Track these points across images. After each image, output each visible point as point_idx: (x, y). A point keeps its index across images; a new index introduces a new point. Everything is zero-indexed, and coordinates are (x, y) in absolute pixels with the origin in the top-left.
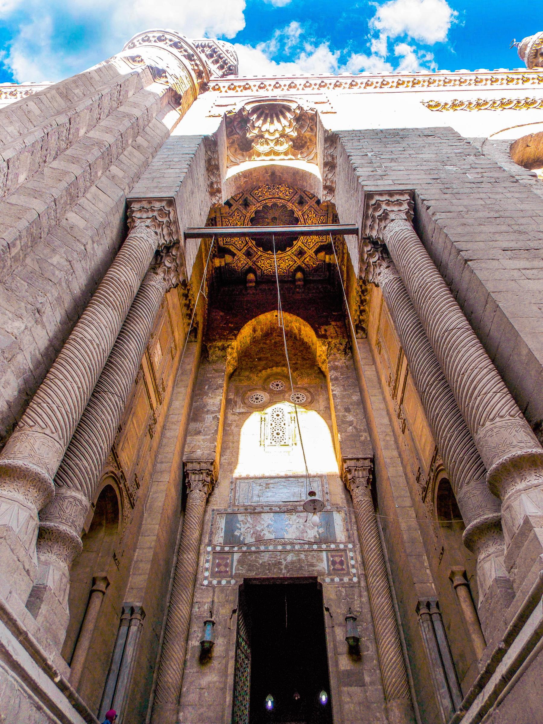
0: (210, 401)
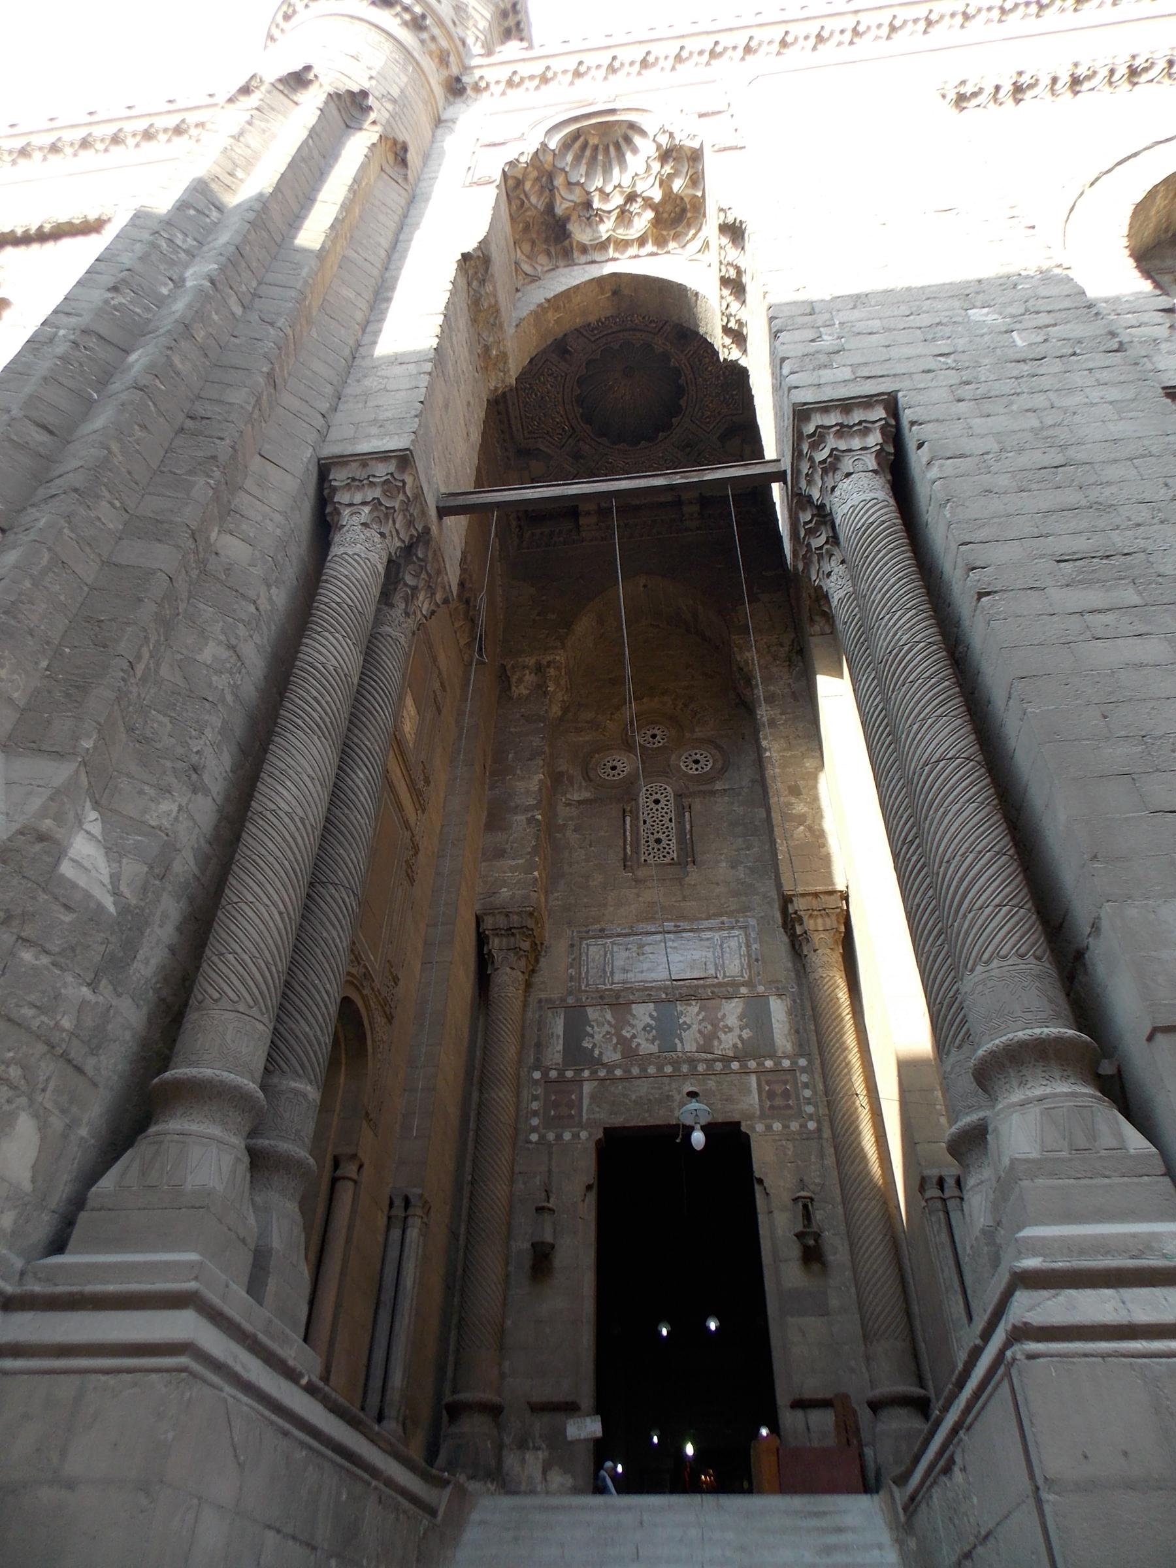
0: (520, 786)
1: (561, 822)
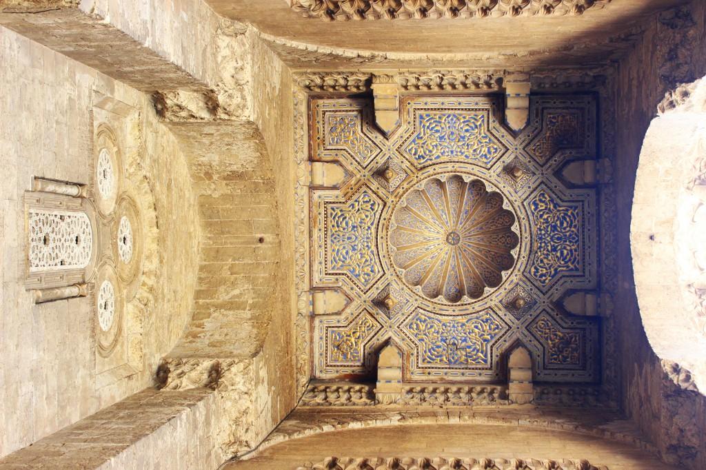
1: (78, 77)
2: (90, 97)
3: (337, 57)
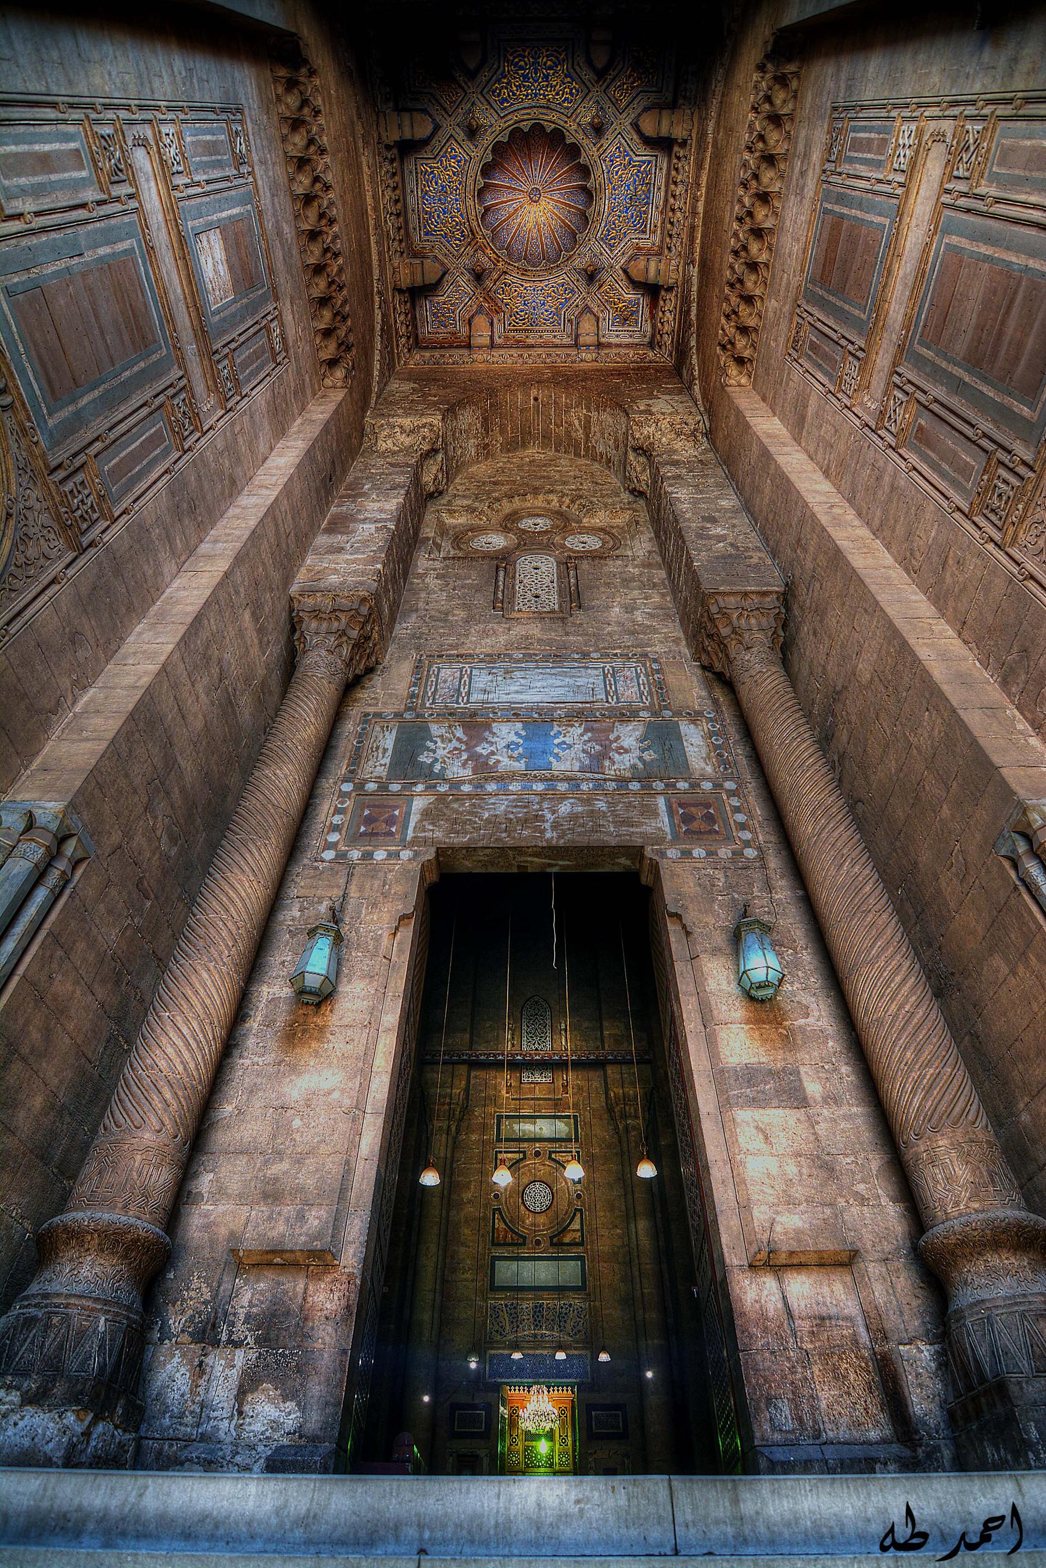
1: (420, 571)
2: (434, 560)
3: (382, 329)
